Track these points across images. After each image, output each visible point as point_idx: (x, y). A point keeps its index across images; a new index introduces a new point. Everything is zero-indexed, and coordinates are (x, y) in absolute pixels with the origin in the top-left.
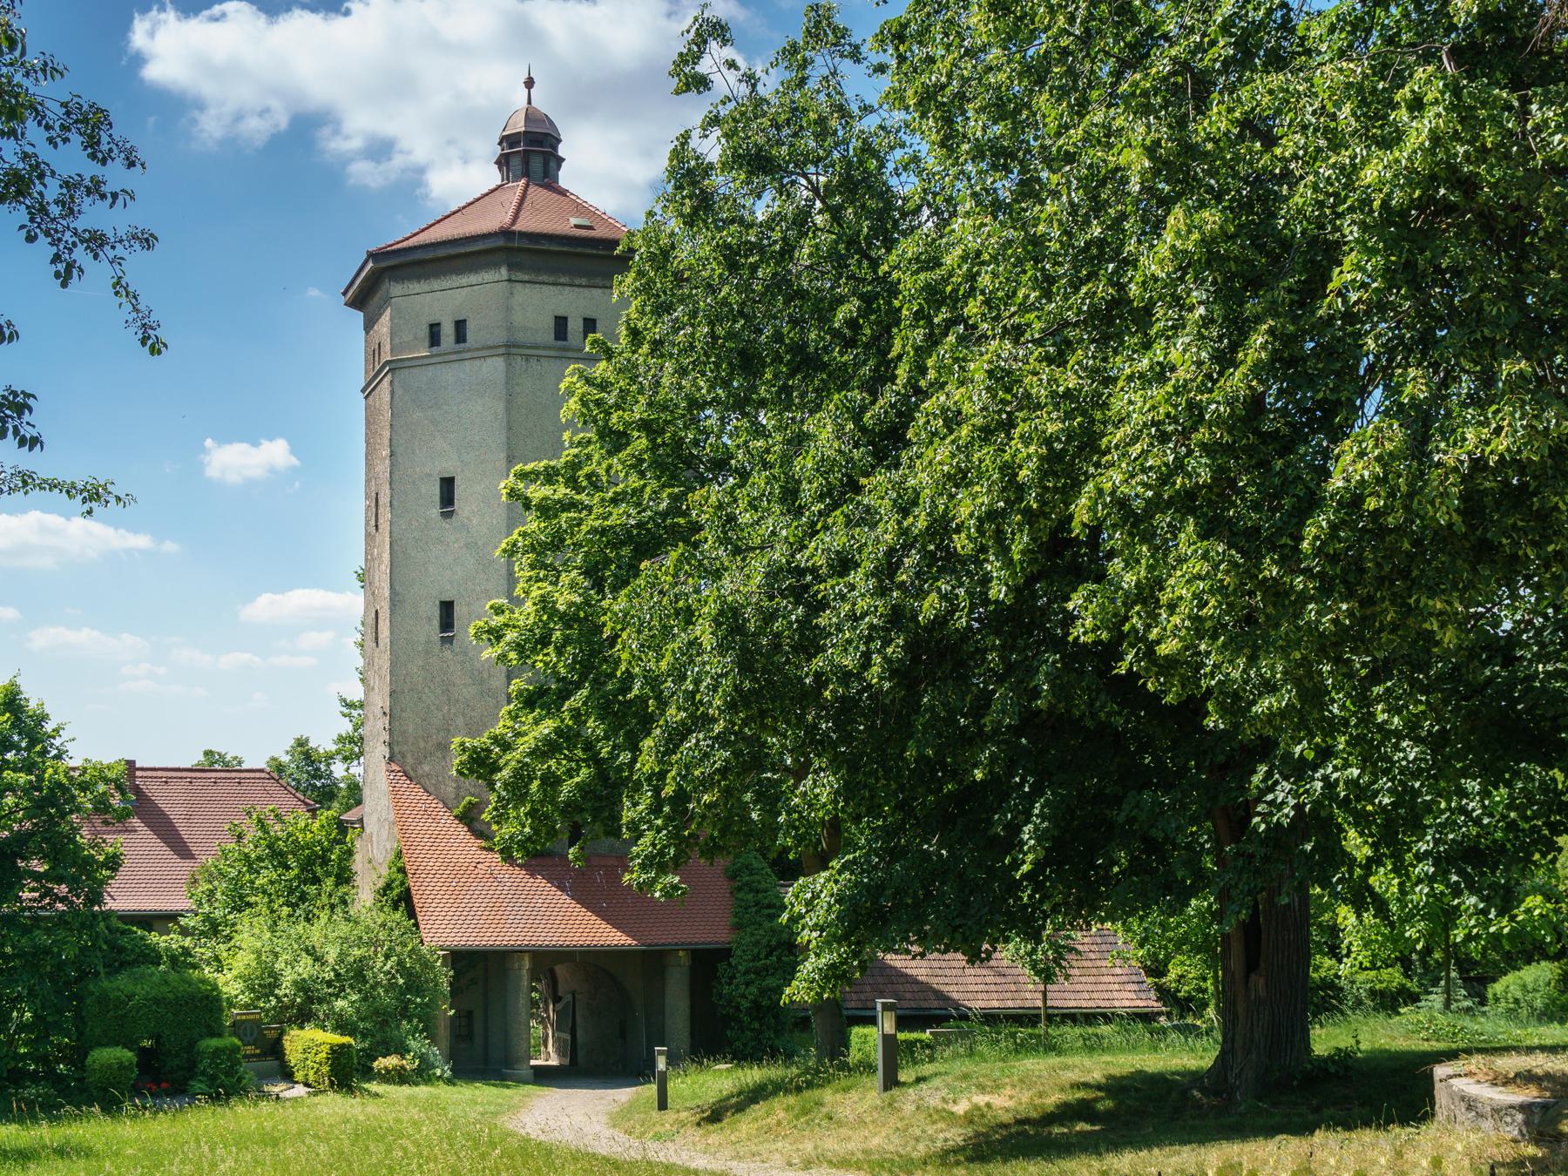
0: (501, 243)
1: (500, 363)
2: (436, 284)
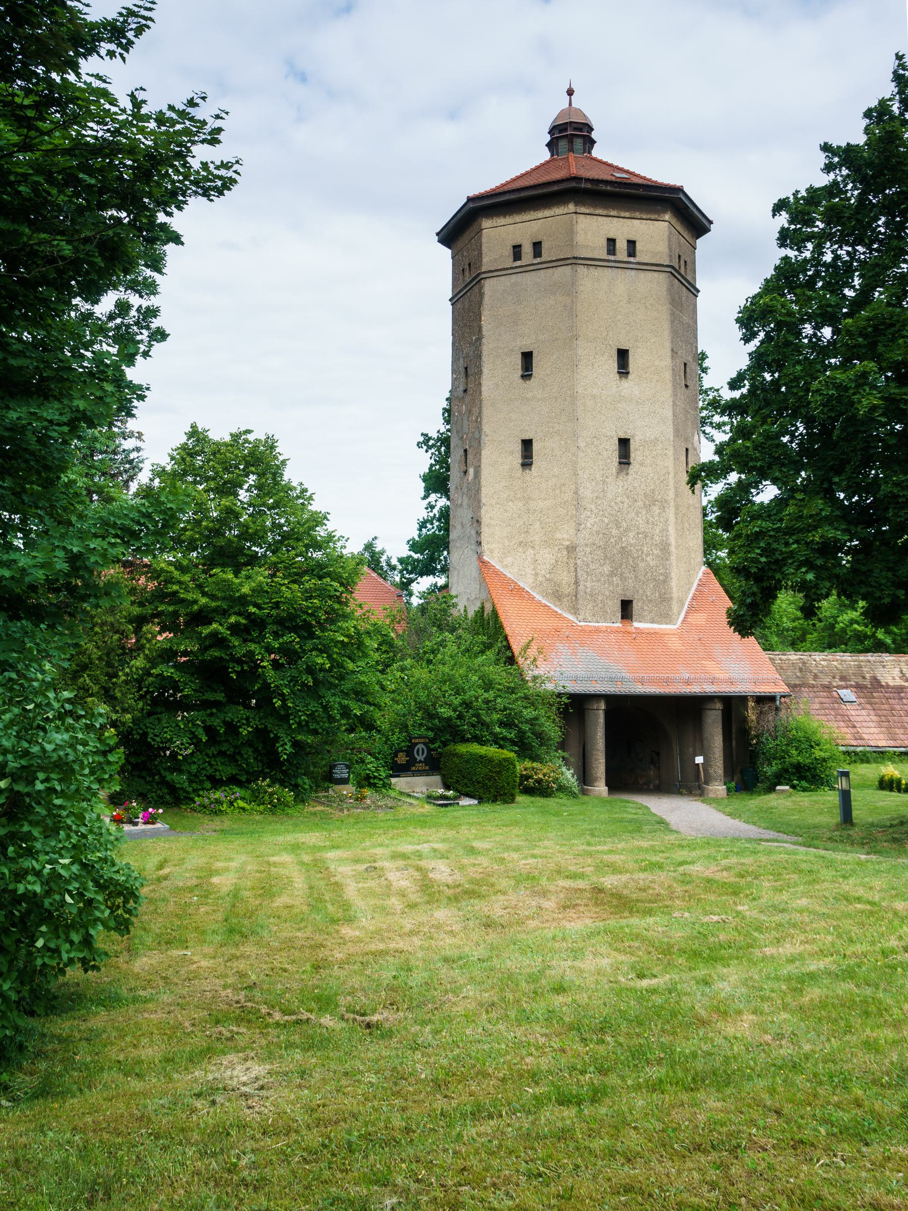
2: (518, 218)
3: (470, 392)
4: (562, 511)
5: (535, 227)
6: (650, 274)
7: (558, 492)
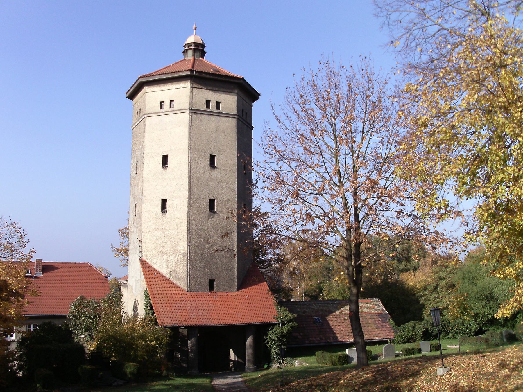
4: (181, 236)
7: (179, 226)
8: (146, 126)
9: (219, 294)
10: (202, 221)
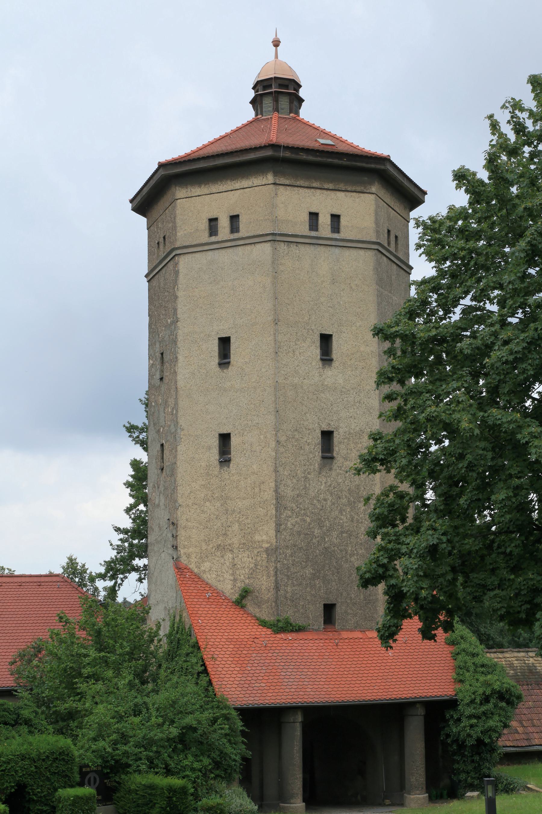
0: (269, 153)
1: (267, 248)
2: (214, 188)
3: (166, 380)
4: (261, 511)
5: (233, 197)
6: (354, 252)
7: (257, 490)
8: (181, 276)
9: (345, 635)
10: (306, 478)
